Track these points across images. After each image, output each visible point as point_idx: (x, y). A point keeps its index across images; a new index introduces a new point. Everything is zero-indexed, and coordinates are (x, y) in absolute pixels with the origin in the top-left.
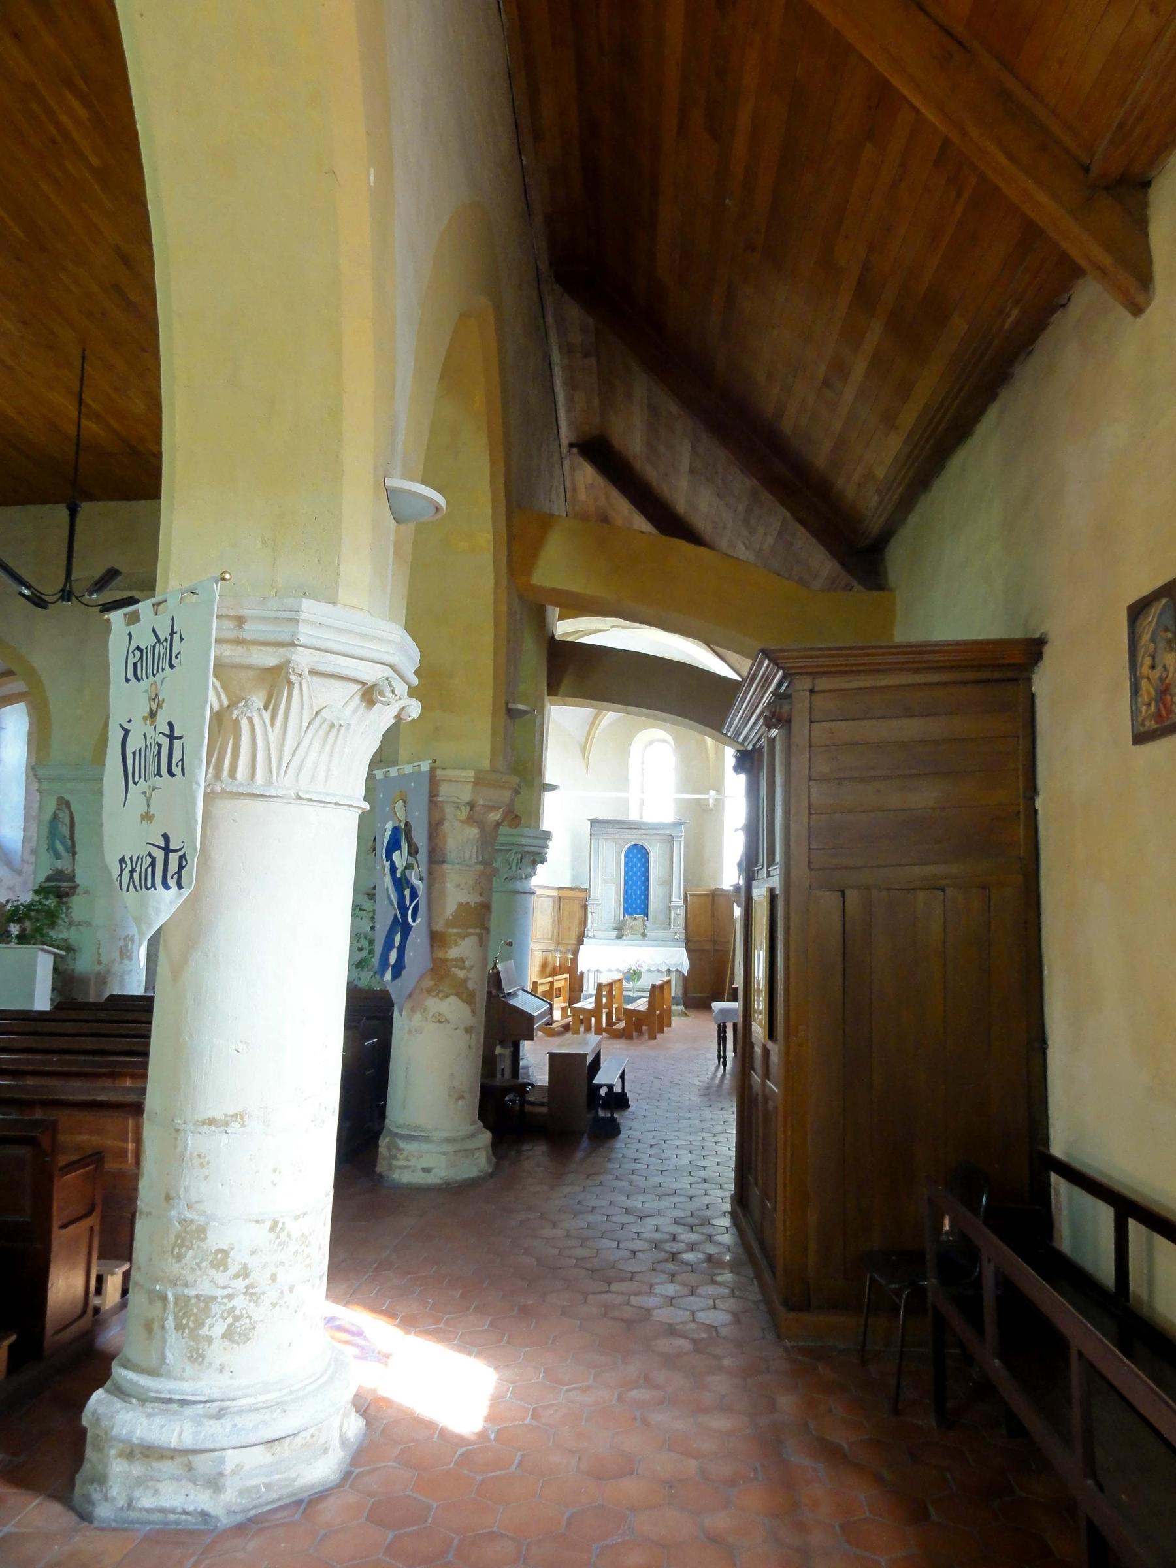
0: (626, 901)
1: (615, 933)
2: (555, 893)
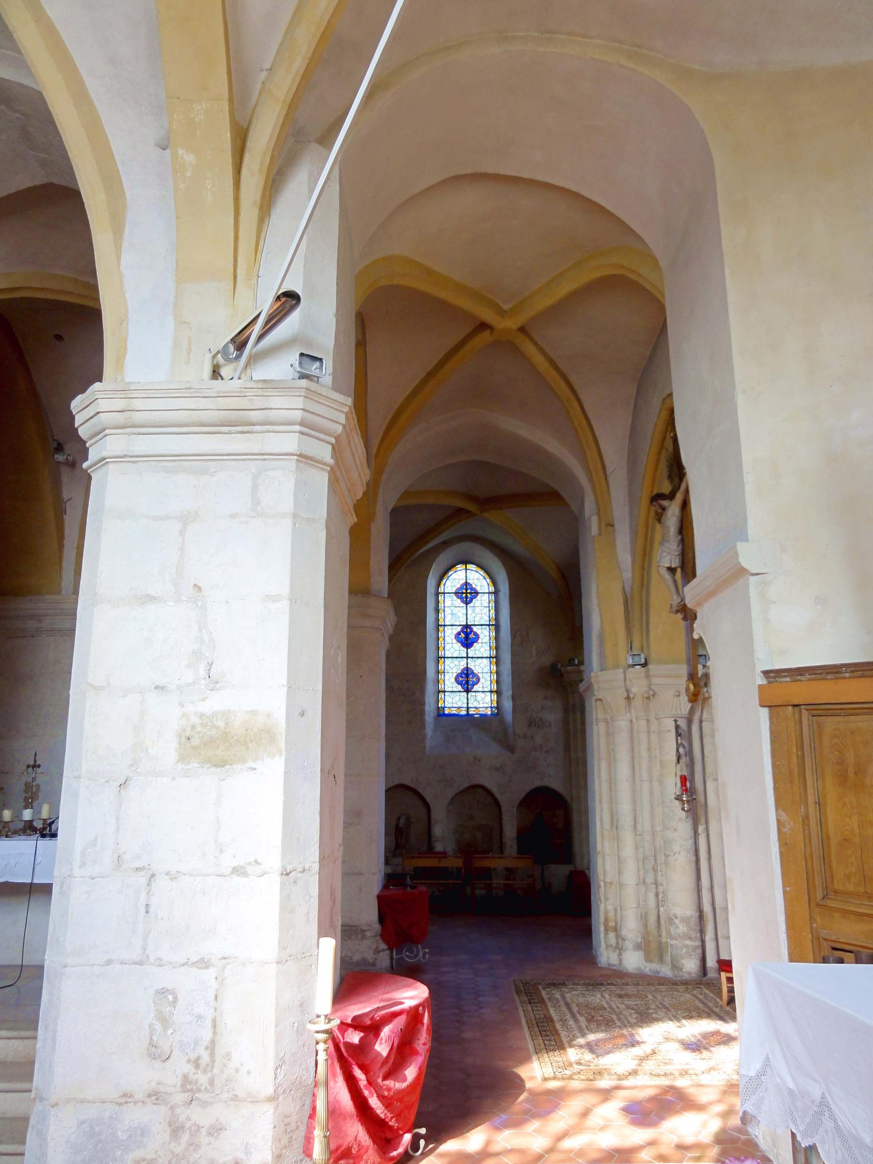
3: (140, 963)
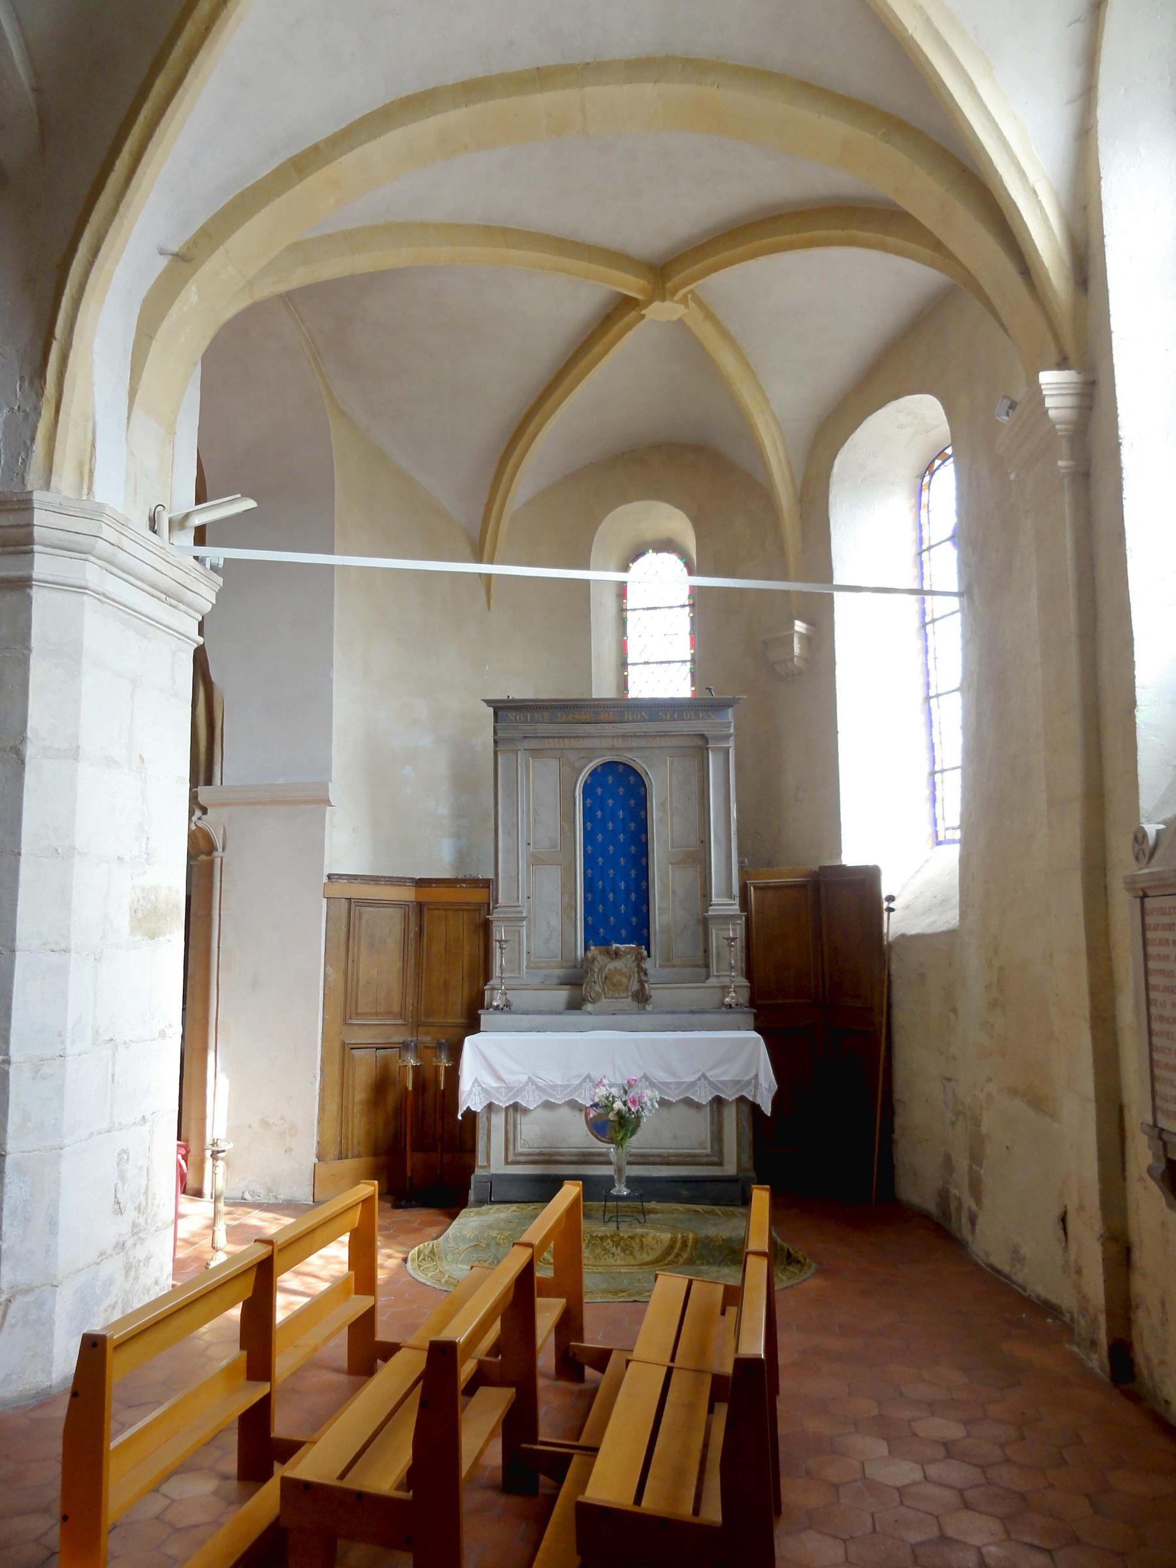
2: (407, 894)
3: (109, 1131)
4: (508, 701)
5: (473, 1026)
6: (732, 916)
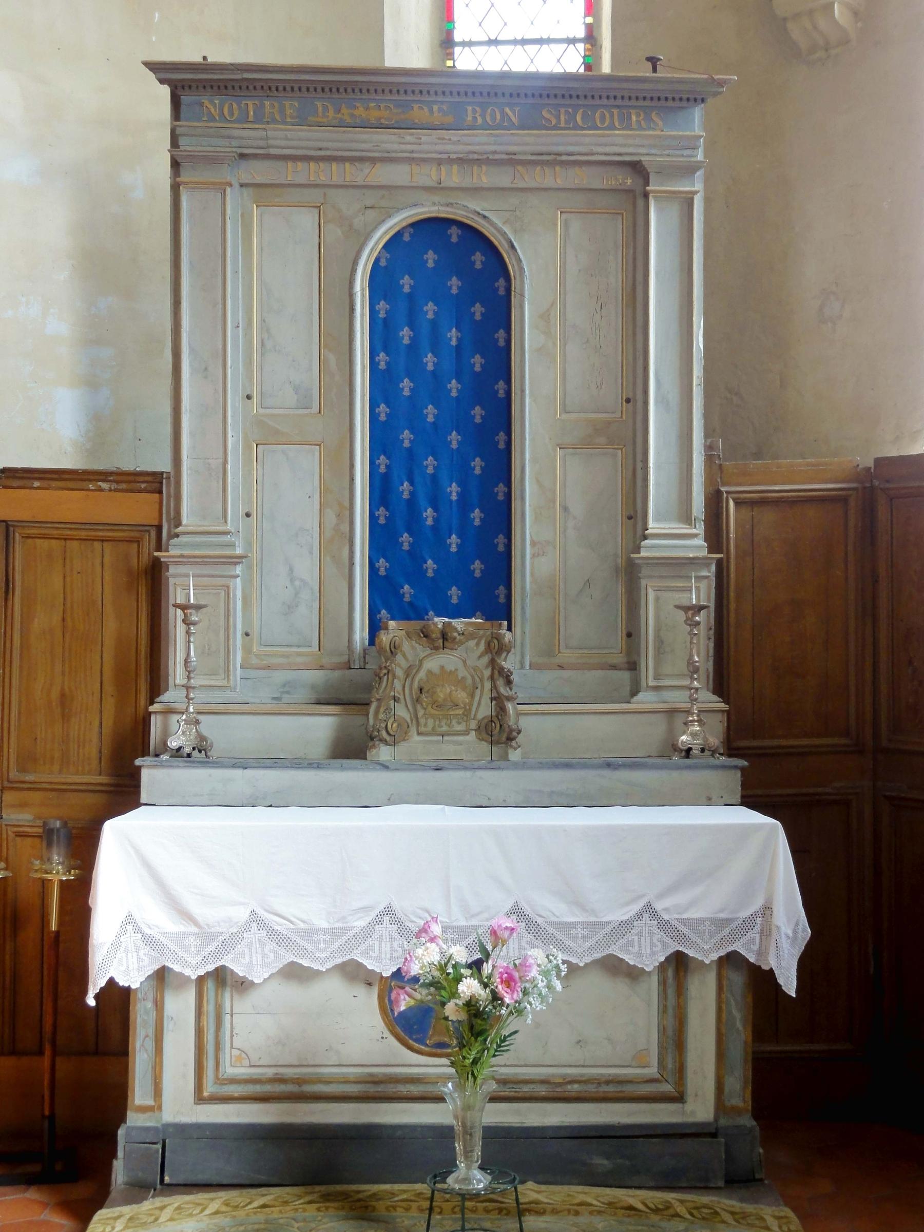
0: (381, 538)
1: (322, 727)
4: (204, 67)
5: (124, 794)
6: (692, 561)
